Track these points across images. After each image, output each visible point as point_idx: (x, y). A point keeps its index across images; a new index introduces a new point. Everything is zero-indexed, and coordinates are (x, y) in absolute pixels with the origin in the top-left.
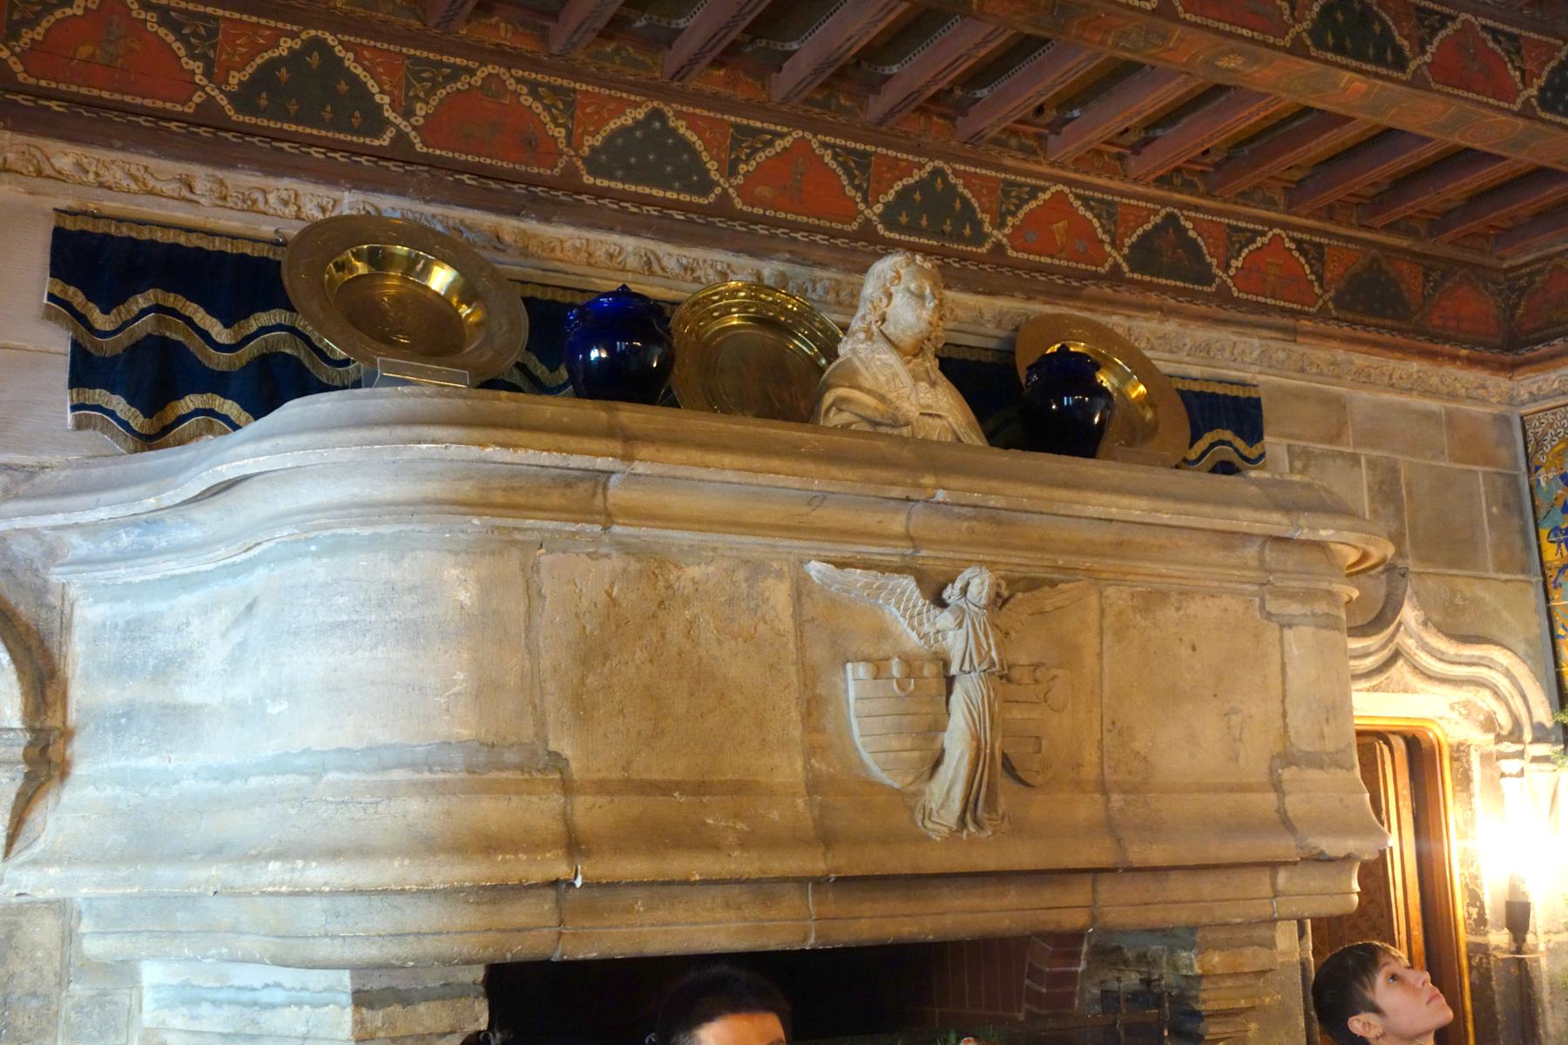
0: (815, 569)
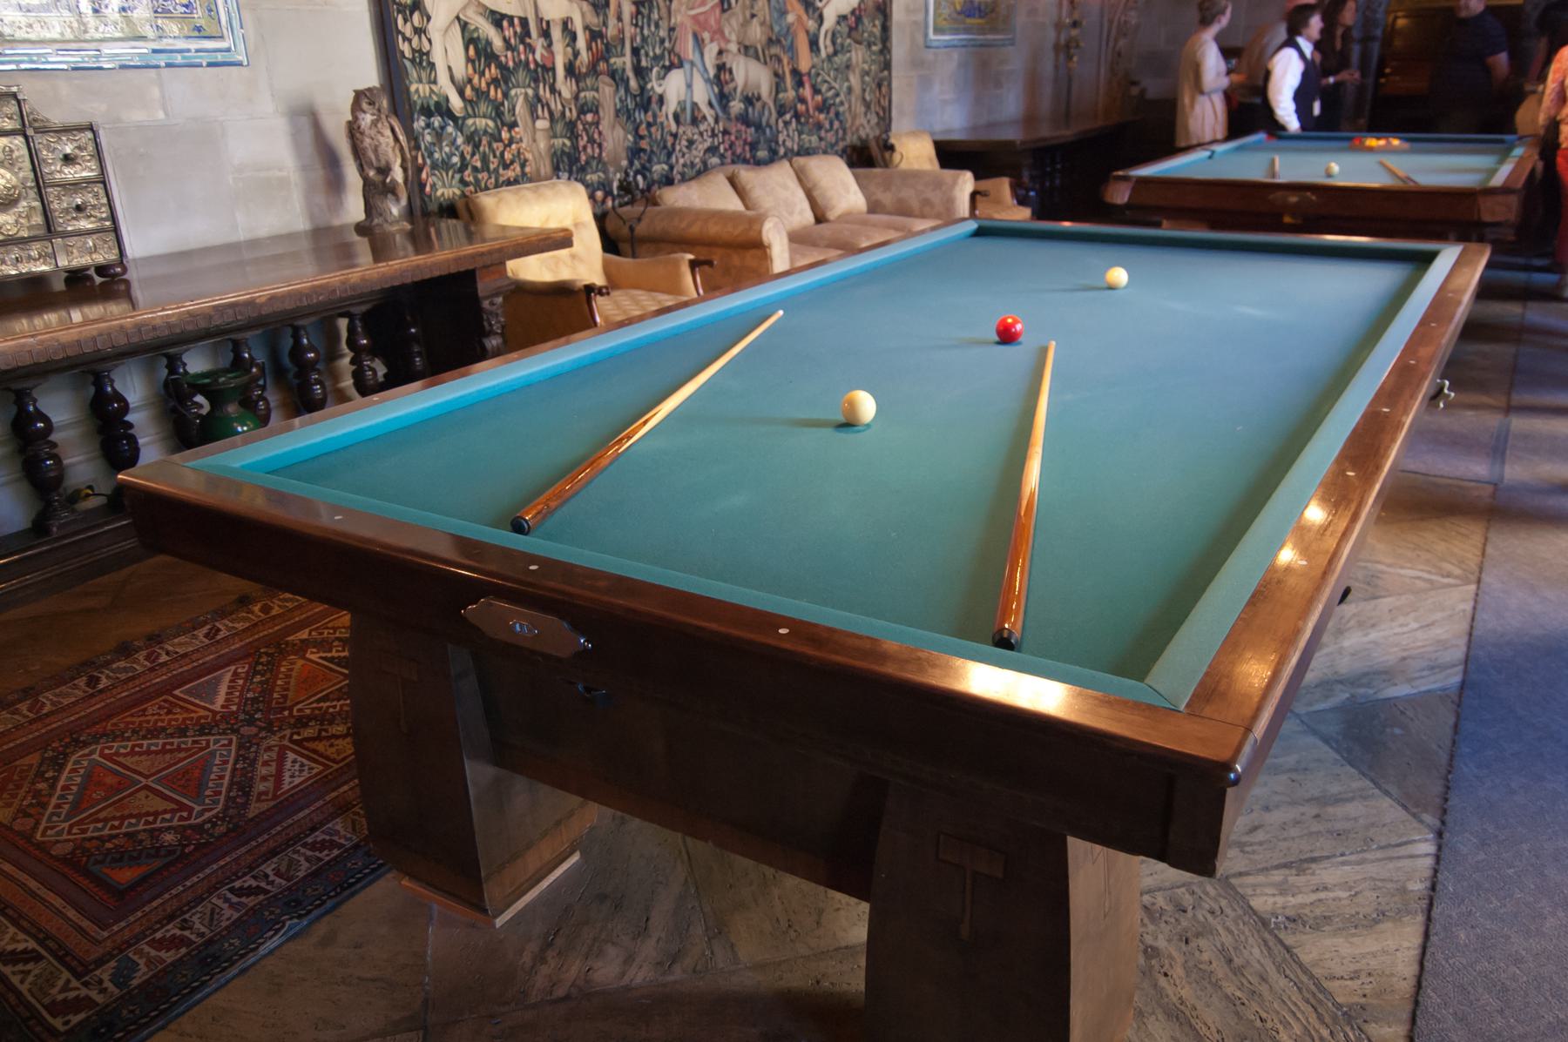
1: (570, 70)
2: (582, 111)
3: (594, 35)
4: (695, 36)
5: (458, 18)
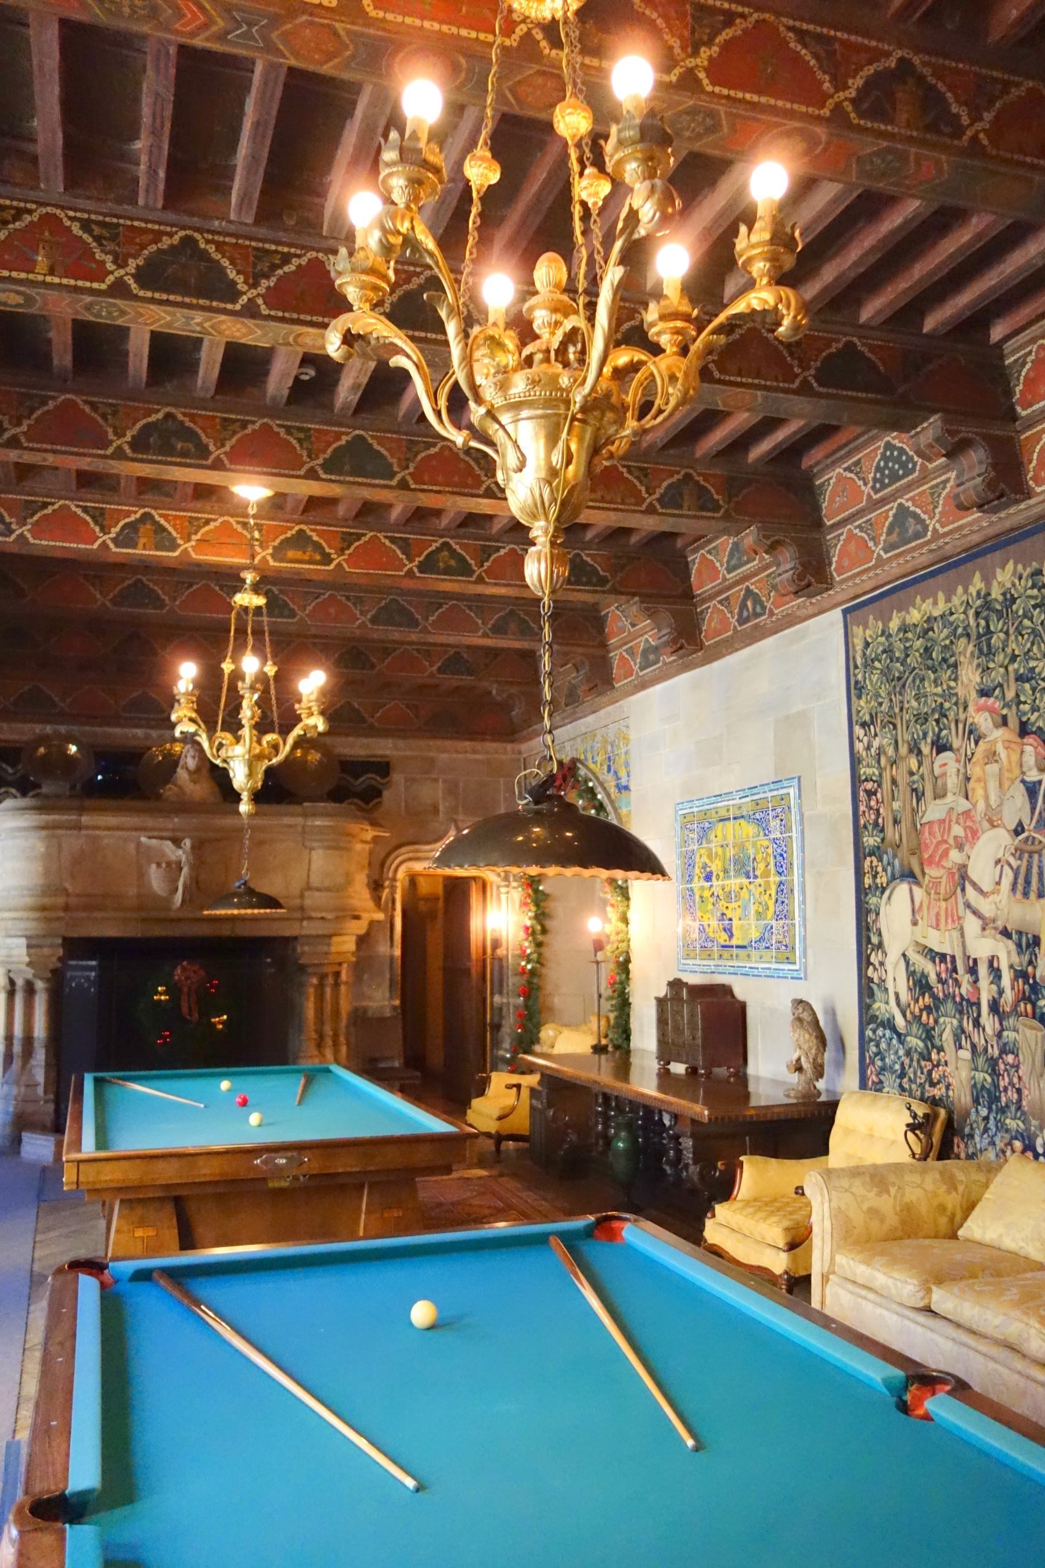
0: (143, 839)
1: (995, 1007)
2: (1004, 1051)
3: (1021, 975)
5: (904, 955)
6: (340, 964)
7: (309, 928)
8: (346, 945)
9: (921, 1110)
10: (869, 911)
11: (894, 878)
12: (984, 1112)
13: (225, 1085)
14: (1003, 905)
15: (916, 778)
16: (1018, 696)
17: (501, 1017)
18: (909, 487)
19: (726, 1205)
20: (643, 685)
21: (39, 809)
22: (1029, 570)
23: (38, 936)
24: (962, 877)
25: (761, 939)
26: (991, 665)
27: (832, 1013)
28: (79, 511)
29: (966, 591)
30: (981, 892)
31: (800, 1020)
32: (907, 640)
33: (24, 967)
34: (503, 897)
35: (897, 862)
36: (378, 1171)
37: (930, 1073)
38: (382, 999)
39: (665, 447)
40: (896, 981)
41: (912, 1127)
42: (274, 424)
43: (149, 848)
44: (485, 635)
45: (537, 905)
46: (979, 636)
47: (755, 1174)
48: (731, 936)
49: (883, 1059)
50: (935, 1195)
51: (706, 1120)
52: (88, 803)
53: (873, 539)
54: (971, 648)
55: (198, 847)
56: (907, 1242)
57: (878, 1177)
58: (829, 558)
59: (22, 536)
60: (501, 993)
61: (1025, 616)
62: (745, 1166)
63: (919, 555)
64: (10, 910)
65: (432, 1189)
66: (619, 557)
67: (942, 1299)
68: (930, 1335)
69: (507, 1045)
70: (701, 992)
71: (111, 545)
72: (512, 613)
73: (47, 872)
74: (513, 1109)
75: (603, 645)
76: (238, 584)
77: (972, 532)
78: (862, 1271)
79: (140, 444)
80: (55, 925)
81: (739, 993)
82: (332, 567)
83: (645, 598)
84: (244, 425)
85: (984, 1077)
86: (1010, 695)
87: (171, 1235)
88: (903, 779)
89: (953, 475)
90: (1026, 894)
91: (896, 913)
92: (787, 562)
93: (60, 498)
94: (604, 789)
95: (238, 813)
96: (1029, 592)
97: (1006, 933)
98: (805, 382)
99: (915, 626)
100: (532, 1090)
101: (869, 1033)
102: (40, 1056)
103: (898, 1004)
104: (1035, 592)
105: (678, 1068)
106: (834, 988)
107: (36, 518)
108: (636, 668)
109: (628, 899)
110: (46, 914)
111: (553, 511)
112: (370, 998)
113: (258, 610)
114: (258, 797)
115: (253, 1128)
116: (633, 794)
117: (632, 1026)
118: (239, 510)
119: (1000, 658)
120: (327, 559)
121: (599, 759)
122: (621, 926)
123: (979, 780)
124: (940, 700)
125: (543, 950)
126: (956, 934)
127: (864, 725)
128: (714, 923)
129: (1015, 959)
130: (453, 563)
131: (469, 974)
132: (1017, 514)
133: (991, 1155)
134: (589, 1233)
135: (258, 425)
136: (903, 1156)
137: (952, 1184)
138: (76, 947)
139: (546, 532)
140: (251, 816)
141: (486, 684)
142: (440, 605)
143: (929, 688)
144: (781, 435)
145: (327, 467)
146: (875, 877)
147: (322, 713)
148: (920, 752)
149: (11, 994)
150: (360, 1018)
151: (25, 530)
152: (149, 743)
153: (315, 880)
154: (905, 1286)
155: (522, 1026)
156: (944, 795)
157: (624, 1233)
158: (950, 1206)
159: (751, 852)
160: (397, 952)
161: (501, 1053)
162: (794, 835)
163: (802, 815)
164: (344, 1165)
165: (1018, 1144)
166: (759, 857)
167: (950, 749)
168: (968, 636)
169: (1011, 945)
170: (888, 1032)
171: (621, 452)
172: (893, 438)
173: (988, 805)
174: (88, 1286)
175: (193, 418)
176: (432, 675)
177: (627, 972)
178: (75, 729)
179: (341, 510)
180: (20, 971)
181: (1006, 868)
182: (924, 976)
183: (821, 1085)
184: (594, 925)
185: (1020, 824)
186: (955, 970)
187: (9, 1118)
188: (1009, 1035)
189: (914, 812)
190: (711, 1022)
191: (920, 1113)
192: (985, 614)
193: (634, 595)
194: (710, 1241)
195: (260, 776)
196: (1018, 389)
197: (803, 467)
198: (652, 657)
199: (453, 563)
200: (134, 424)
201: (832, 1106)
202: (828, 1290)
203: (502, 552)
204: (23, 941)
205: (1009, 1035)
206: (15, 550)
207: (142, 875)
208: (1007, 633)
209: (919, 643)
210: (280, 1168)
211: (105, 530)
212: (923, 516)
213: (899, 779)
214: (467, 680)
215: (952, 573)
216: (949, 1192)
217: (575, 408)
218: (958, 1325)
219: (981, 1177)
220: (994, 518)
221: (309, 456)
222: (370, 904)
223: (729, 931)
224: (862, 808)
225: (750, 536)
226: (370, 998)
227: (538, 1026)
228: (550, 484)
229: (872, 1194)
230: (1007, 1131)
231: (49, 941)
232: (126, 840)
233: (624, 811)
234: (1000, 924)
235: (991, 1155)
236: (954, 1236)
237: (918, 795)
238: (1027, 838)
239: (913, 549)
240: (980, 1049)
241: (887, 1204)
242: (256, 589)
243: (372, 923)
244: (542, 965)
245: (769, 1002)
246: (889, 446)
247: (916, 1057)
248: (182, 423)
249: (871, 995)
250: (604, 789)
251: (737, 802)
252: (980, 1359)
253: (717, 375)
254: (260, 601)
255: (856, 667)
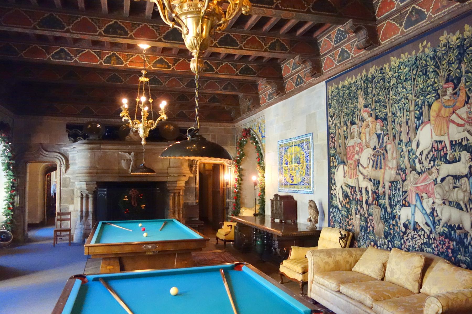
1: (367, 202)
2: (369, 215)
3: (374, 192)
4: (418, 194)
6: (180, 190)
7: (170, 179)
8: (182, 184)
9: (344, 233)
10: (332, 173)
11: (339, 163)
12: (363, 234)
13: (140, 225)
14: (369, 171)
15: (346, 133)
16: (375, 107)
17: (229, 205)
18: (345, 42)
19: (286, 261)
20: (269, 105)
21: (89, 144)
22: (379, 68)
23: (89, 181)
24: (358, 163)
25: (302, 182)
26: (368, 98)
27: (321, 204)
28: (93, 53)
29: (361, 75)
30: (364, 167)
31: (311, 206)
32: (344, 90)
33: (85, 190)
34: (229, 170)
35: (340, 159)
36: (179, 250)
37: (348, 222)
38: (193, 200)
39: (270, 31)
40: (339, 194)
41: (341, 238)
42: (148, 25)
43: (121, 155)
44: (221, 90)
45: (239, 172)
46: (365, 89)
47: (295, 252)
48: (293, 181)
49: (335, 218)
50: (346, 258)
51: (281, 236)
52: (102, 141)
53: (334, 59)
54: (362, 92)
55: (136, 155)
56: (336, 272)
57: (329, 252)
58: (322, 65)
59: (76, 60)
60: (229, 198)
61: (378, 82)
62: (292, 249)
63: (347, 64)
64: (80, 174)
65: (201, 255)
66: (260, 66)
67: (343, 289)
68: (340, 299)
69: (230, 214)
70: (282, 198)
71: (103, 63)
72: (229, 83)
73: (91, 162)
74: (230, 232)
75: (257, 93)
76: (141, 75)
77: (363, 56)
78: (321, 280)
79: (106, 31)
80: (94, 178)
81: (295, 198)
82: (171, 69)
83: (268, 78)
84: (139, 25)
85: (363, 223)
86: (373, 107)
87: (118, 268)
88: (342, 133)
89: (357, 38)
90: (376, 168)
91: (339, 174)
92: (309, 66)
93: (87, 49)
94: (258, 137)
95: (141, 144)
96: (379, 75)
97: (370, 180)
98: (309, 9)
99: (346, 86)
100: (235, 227)
101: (331, 210)
102: (91, 216)
103: (340, 201)
104: (381, 75)
105: (277, 221)
106: (321, 197)
107: (80, 55)
108: (267, 100)
109: (264, 170)
110: (92, 175)
111: (198, 47)
112: (189, 200)
113: (147, 82)
114: (147, 139)
115: (145, 237)
116: (266, 138)
117: (265, 208)
118: (140, 51)
119: (370, 96)
120: (169, 67)
121: (257, 128)
122: (262, 178)
123: (364, 133)
124: (353, 109)
125: (241, 186)
126: (356, 180)
127: (331, 117)
128: (288, 177)
129: (373, 188)
130: (208, 68)
131: (219, 193)
132: (376, 50)
133: (365, 246)
134: (233, 268)
135: (143, 25)
136: (338, 246)
137: (351, 255)
138: (100, 185)
139: (196, 53)
140: (145, 145)
141: (223, 105)
142: (207, 81)
143: (350, 105)
144: (306, 27)
145: (165, 38)
146: (333, 163)
147: (165, 114)
148: (347, 125)
149: (82, 198)
150: (186, 206)
151: (77, 59)
152: (122, 124)
153: (172, 165)
154: (332, 284)
155: (235, 208)
156: (354, 138)
157: (242, 268)
158: (350, 261)
159: (299, 156)
160: (197, 186)
161: (229, 216)
162: (311, 150)
163: (313, 144)
164: (169, 248)
165: (372, 243)
166: (301, 157)
167: (356, 124)
168: (361, 89)
169: (372, 183)
170: (336, 210)
171: (224, 29)
172: (340, 27)
173: (366, 141)
174: (78, 282)
175: (123, 23)
176: (206, 103)
177: (264, 192)
178: (100, 120)
179: (173, 52)
180: (84, 192)
181: (371, 160)
182: (347, 193)
183: (317, 225)
184: (254, 178)
185: (375, 147)
186: (356, 191)
187: (82, 235)
188: (371, 211)
189: (345, 143)
190: (287, 206)
191: (343, 234)
192: (366, 82)
193: (264, 77)
194: (281, 271)
195: (147, 133)
196: (377, 11)
197: (314, 37)
198: (271, 97)
199: (208, 68)
200: (105, 25)
201: (320, 231)
202: (312, 286)
203: (223, 64)
204: (85, 183)
205: (371, 211)
206: (74, 65)
207: (119, 163)
208: (372, 88)
209: (347, 91)
210: (149, 249)
211: (101, 58)
212: (349, 52)
213: (341, 133)
214: (217, 104)
215: (357, 69)
216: (350, 257)
217: (203, 14)
218: (347, 296)
219: (359, 252)
220: (369, 52)
221: (159, 34)
222: (189, 172)
223: (292, 179)
224: (330, 142)
225: (297, 58)
226: (189, 200)
227: (240, 208)
228: (197, 38)
229: (326, 258)
230: (370, 239)
231: (92, 183)
232: (114, 153)
233: (263, 144)
234: (369, 177)
235: (365, 246)
236: (351, 270)
237: (346, 138)
238: (377, 151)
239: (346, 62)
240: (362, 215)
241: (331, 261)
242: (146, 76)
243: (190, 177)
244: (241, 190)
245: (302, 200)
246: (339, 30)
247: (344, 217)
248: (120, 24)
249: (332, 198)
250: (258, 137)
251: (295, 140)
252: (353, 306)
253: (280, 7)
254: (147, 80)
255: (329, 99)
